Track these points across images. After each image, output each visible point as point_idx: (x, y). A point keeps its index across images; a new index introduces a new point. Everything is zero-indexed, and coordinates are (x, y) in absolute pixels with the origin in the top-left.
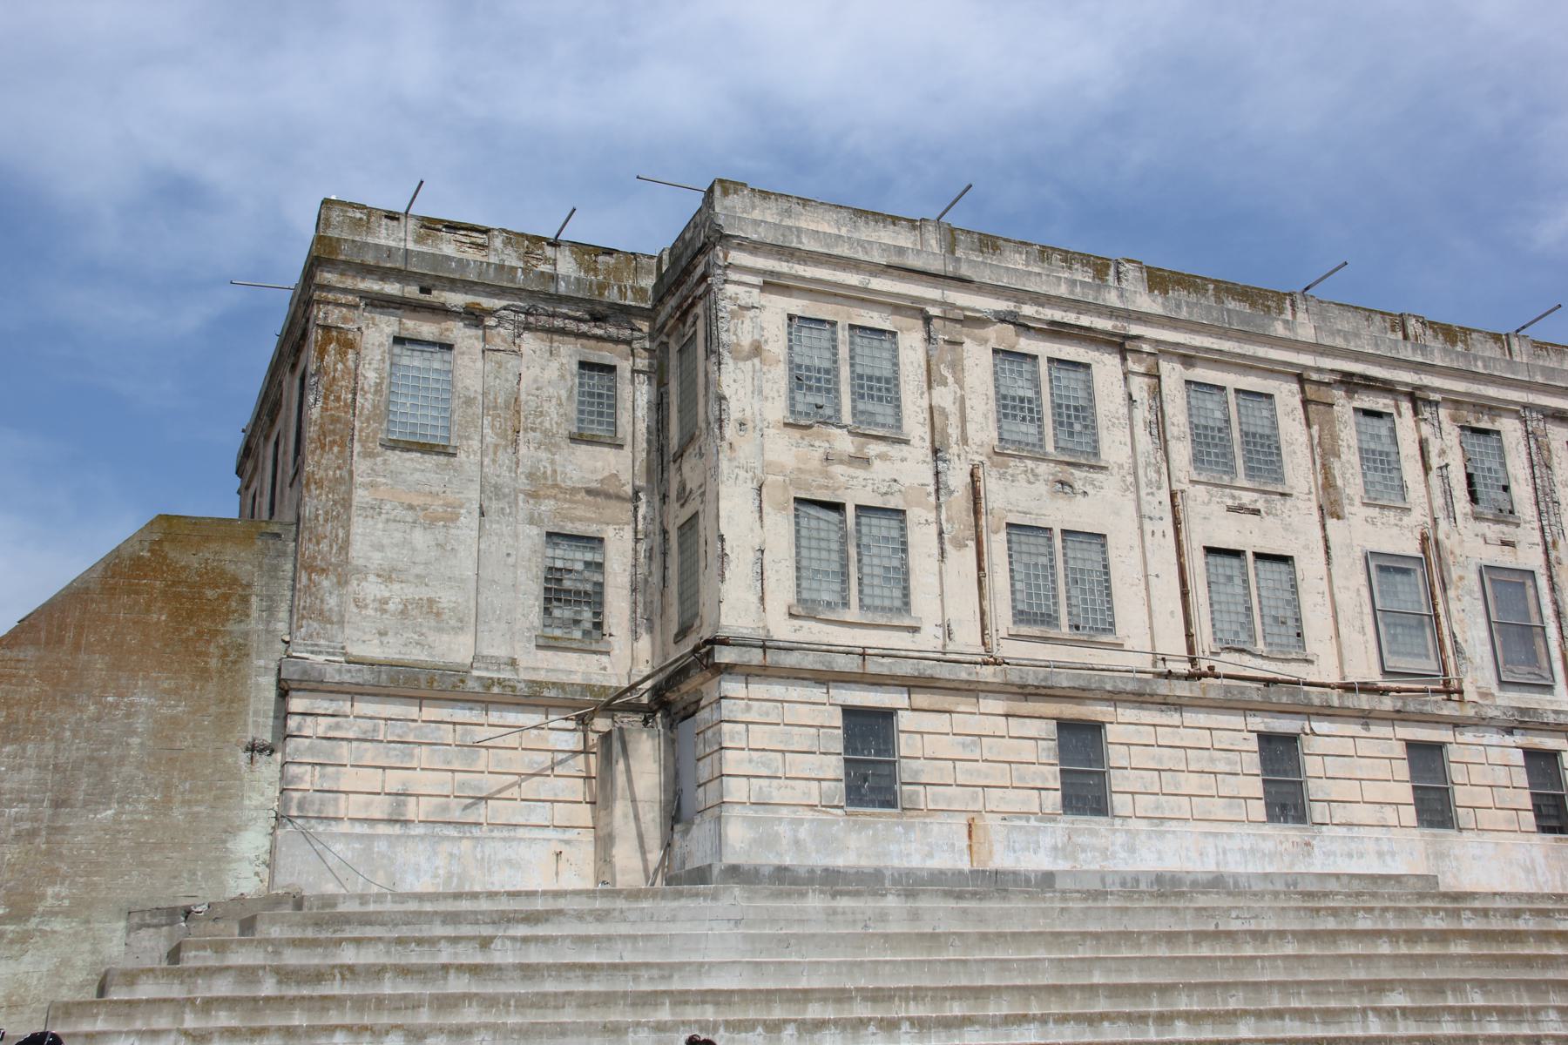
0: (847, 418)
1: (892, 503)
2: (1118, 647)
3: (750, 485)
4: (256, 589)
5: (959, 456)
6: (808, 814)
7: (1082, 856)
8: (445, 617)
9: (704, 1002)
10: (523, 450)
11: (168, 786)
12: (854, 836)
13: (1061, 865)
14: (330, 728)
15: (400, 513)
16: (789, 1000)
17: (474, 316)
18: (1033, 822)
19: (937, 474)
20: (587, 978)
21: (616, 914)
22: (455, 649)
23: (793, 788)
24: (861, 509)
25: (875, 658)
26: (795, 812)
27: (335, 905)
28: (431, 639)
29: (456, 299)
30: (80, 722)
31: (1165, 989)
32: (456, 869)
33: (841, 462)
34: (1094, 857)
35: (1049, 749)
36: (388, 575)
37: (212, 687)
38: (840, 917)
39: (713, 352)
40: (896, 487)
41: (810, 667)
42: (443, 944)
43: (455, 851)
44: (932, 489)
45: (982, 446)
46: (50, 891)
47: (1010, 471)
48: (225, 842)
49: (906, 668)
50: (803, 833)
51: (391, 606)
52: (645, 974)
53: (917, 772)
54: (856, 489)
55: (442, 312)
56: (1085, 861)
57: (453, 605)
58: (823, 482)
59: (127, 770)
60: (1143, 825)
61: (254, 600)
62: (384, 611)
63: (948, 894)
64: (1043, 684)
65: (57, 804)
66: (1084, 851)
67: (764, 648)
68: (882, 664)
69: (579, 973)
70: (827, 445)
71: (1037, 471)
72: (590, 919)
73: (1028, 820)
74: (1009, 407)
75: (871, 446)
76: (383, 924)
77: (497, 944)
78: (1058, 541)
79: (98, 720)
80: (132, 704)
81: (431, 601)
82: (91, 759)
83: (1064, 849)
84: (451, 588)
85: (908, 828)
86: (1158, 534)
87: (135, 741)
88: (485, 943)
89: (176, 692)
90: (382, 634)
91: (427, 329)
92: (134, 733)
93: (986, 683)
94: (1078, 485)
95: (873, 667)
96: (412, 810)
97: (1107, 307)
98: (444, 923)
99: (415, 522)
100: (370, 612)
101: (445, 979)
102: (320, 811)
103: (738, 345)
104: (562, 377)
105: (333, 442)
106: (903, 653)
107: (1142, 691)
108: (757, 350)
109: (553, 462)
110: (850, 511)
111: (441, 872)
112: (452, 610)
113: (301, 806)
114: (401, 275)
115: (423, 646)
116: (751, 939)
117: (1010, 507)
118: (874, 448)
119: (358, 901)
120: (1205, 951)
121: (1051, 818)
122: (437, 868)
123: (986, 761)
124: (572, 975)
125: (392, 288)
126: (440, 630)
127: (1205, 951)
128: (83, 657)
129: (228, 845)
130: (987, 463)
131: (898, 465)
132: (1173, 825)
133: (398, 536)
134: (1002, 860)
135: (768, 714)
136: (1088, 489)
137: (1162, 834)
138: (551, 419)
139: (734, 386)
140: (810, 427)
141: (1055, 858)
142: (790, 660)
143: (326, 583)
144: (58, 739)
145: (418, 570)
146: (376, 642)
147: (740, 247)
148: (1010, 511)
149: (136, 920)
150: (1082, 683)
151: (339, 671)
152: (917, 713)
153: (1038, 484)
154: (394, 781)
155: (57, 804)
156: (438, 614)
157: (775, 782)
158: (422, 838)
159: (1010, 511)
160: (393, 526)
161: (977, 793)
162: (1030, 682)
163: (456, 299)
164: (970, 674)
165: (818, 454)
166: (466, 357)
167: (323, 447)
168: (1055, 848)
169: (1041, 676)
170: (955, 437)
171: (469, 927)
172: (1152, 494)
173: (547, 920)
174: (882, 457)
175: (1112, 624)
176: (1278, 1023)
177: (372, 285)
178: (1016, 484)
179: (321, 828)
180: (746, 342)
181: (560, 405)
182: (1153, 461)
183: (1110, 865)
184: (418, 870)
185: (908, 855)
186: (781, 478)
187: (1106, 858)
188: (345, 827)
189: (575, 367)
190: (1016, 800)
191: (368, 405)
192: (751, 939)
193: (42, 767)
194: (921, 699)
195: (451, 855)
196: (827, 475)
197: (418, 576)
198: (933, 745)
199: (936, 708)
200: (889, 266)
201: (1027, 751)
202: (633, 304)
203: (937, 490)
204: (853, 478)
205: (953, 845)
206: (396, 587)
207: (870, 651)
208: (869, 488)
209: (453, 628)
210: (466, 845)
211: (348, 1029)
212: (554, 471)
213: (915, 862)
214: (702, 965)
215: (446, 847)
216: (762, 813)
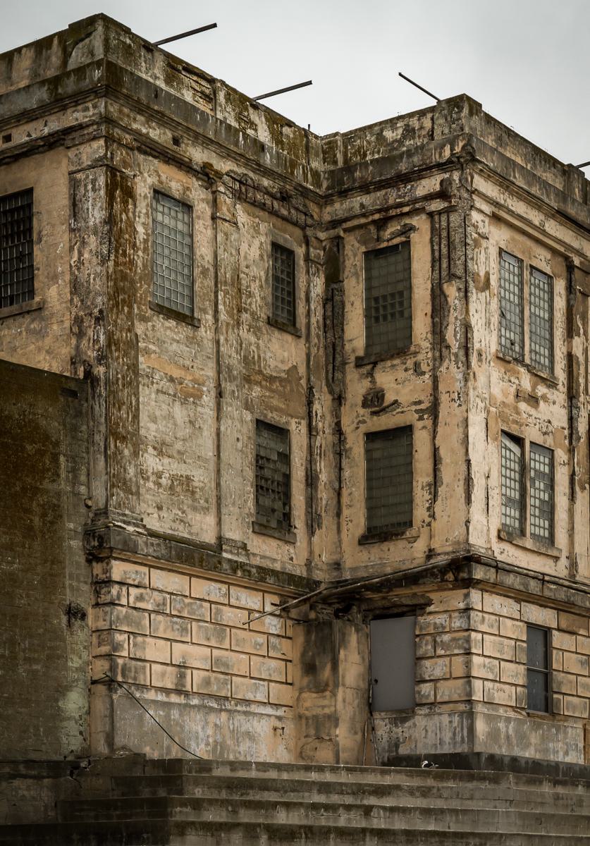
8: (197, 496)
15: (165, 384)
21: (435, 791)
27: (210, 770)
28: (190, 517)
36: (161, 449)
38: (561, 802)
41: (518, 588)
42: (341, 810)
48: (57, 700)
51: (164, 481)
57: (202, 485)
62: (159, 485)
67: (497, 568)
72: (418, 794)
76: (276, 790)
77: (374, 813)
81: (188, 478)
84: (200, 467)
90: (160, 508)
98: (320, 792)
99: (175, 396)
100: (151, 485)
101: (364, 840)
102: (135, 679)
104: (261, 256)
109: (258, 347)
112: (202, 489)
115: (185, 523)
116: (522, 816)
119: (228, 768)
122: (208, 737)
124: (433, 840)
126: (195, 509)
129: (60, 704)
138: (256, 301)
142: (510, 580)
145: (179, 446)
146: (156, 515)
156: (193, 493)
157: (497, 685)
171: (336, 796)
173: (389, 794)
181: (261, 287)
184: (197, 738)
188: (151, 695)
189: (269, 248)
192: (522, 816)
202: (312, 187)
209: (203, 508)
212: (259, 357)
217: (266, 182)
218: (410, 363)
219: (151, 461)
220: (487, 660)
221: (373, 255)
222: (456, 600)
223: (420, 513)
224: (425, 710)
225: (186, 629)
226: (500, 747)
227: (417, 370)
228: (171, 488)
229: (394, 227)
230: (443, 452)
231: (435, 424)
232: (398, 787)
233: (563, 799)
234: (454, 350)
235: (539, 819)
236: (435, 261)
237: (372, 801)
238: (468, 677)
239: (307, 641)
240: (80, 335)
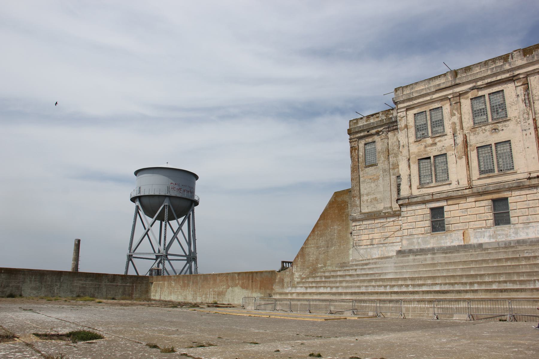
0: (430, 134)
1: (443, 152)
2: (515, 173)
3: (406, 160)
4: (349, 203)
5: (460, 134)
6: (421, 236)
7: (499, 237)
9: (380, 281)
10: (390, 159)
11: (340, 242)
12: (432, 240)
13: (492, 240)
14: (359, 228)
15: (369, 181)
16: (395, 280)
17: (377, 133)
18: (483, 230)
19: (454, 140)
20: (367, 276)
22: (380, 207)
23: (418, 230)
24: (435, 157)
25: (436, 195)
26: (418, 236)
29: (374, 131)
30: (328, 232)
31: (481, 275)
32: (382, 253)
33: (429, 146)
34: (503, 237)
35: (489, 208)
36: (367, 195)
37: (344, 223)
38: (416, 261)
40: (443, 148)
42: (350, 270)
43: (382, 249)
44: (454, 145)
45: (468, 128)
47: (477, 132)
49: (444, 195)
50: (420, 240)
51: (369, 201)
52: (376, 275)
53: (449, 221)
54: (433, 152)
55: (372, 135)
56: (500, 238)
58: (425, 153)
59: (335, 240)
60: (522, 226)
61: (349, 204)
63: (443, 253)
64: (485, 191)
66: (499, 235)
68: (437, 196)
69: (366, 275)
70: (425, 143)
71: (486, 129)
73: (482, 229)
74: (475, 113)
75: (436, 139)
77: (357, 270)
78: (493, 148)
79: (331, 232)
80: (335, 228)
81: (376, 198)
82: (330, 239)
83: (493, 236)
85: (446, 236)
86: (528, 134)
87: (335, 235)
88: (356, 270)
89: (339, 225)
90: (368, 207)
91: (370, 140)
92: (335, 233)
93: (467, 194)
94: (500, 128)
95: (435, 197)
96: (375, 242)
97: (505, 70)
103: (401, 127)
105: (355, 170)
106: (443, 192)
107: (519, 185)
108: (406, 127)
109: (397, 160)
110: (432, 158)
111: (380, 254)
113: (355, 244)
114: (363, 131)
116: (395, 267)
117: (477, 142)
118: (437, 140)
120: (509, 263)
121: (489, 227)
123: (469, 215)
125: (362, 134)
126: (378, 203)
127: (509, 263)
128: (328, 221)
130: (470, 132)
131: (444, 142)
132: (533, 224)
133: (369, 185)
134: (473, 241)
135: (412, 214)
136: (504, 128)
137: (528, 228)
139: (401, 137)
140: (421, 140)
141: (490, 238)
143: (356, 199)
144: (326, 236)
145: (373, 192)
146: (367, 209)
147: (400, 103)
148: (478, 143)
150: (497, 188)
151: (358, 216)
152: (449, 206)
153: (486, 133)
154: (371, 236)
155: (327, 247)
156: (377, 200)
157: (414, 229)
158: (376, 247)
159: (478, 143)
160: (368, 184)
161: (466, 224)
162: (480, 191)
163: (374, 131)
164: (462, 193)
165: (423, 146)
166: (378, 143)
167: (353, 172)
168: (490, 236)
169: (483, 189)
170: (458, 129)
172: (526, 122)
174: (440, 141)
175: (513, 166)
176: (505, 284)
177: (359, 135)
178: (479, 135)
179: (359, 248)
180: (403, 125)
182: (526, 111)
183: (509, 239)
185: (446, 243)
186: (414, 156)
187: (507, 237)
188: (363, 247)
190: (478, 224)
191: (361, 160)
192: (395, 267)
193: (325, 241)
194: (450, 202)
195: (381, 250)
196: (425, 151)
197: (373, 193)
198: (453, 214)
199: (454, 204)
200: (436, 91)
201: (482, 210)
203: (455, 145)
204: (432, 149)
205: (459, 239)
206: (369, 196)
207: (434, 193)
208: (436, 151)
210: (384, 248)
211: (323, 286)
213: (448, 244)
214: (386, 273)
215: (380, 249)
216: (410, 237)
220: (409, 224)
225: (373, 231)
226: (414, 246)
228: (371, 201)
232: (370, 263)
233: (417, 259)
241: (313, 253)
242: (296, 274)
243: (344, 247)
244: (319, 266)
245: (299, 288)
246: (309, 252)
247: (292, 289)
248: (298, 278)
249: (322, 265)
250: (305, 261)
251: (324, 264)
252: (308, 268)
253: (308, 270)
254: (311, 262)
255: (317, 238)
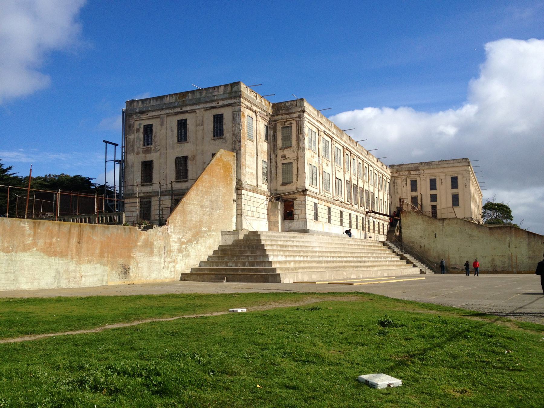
31: (354, 253)
39: (301, 134)
46: (213, 226)
59: (220, 203)
65: (212, 209)
87: (220, 197)
89: (224, 187)
144: (211, 195)
145: (251, 166)
149: (224, 233)
193: (210, 201)
217: (264, 113)
218: (292, 150)
219: (247, 170)
221: (283, 128)
222: (302, 198)
223: (294, 180)
224: (296, 220)
227: (293, 151)
229: (288, 123)
230: (299, 168)
231: (298, 161)
232: (296, 237)
234: (302, 148)
235: (321, 243)
236: (297, 130)
237: (292, 239)
238: (305, 214)
239: (272, 206)
240: (235, 144)
241: (196, 212)
242: (173, 236)
243: (228, 213)
244: (203, 229)
245: (280, 257)
246: (192, 211)
247: (274, 257)
248: (176, 242)
249: (207, 229)
250: (186, 221)
251: (208, 229)
252: (190, 230)
253: (190, 233)
254: (194, 223)
255: (200, 195)
